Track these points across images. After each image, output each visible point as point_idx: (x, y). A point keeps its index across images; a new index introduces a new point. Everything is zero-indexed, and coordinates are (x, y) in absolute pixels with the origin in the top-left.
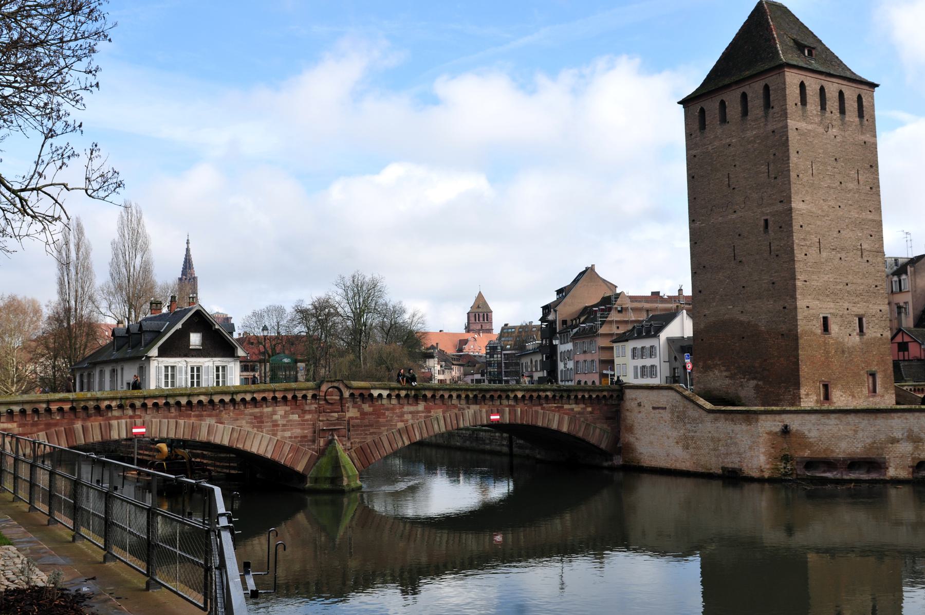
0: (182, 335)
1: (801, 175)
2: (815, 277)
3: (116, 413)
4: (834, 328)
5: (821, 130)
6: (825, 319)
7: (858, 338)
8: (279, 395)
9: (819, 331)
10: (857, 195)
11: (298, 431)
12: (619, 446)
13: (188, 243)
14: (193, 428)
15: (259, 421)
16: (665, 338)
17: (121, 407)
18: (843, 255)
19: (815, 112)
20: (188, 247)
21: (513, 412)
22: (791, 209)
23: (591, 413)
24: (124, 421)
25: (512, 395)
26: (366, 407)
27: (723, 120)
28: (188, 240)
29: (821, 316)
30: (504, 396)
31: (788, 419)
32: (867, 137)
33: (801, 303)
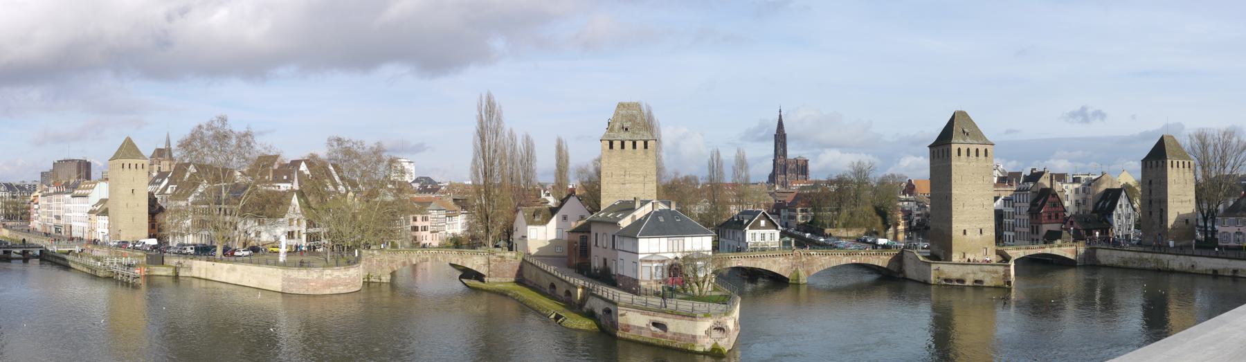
0: (758, 221)
3: (734, 259)
5: (967, 164)
6: (965, 231)
10: (982, 186)
11: (787, 265)
12: (901, 270)
13: (780, 111)
14: (755, 264)
21: (860, 258)
22: (951, 194)
26: (809, 258)
27: (938, 157)
31: (939, 265)
32: (989, 164)
33: (954, 226)
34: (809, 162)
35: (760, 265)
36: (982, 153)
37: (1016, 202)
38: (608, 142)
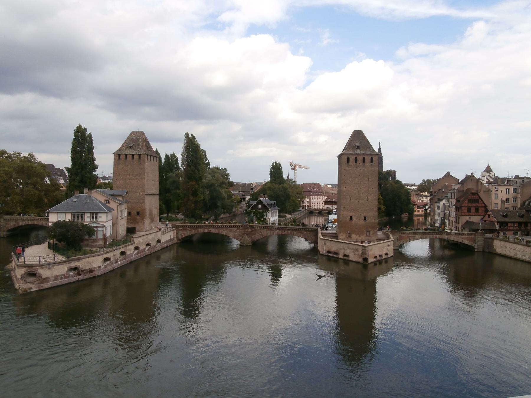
1: (345, 181)
2: (348, 207)
4: (354, 219)
5: (355, 169)
7: (363, 222)
8: (235, 226)
9: (348, 220)
10: (367, 185)
11: (238, 233)
13: (380, 144)
15: (231, 231)
16: (443, 204)
17: (206, 227)
18: (360, 201)
19: (352, 164)
20: (380, 145)
23: (310, 234)
24: (207, 229)
25: (287, 229)
26: (253, 229)
28: (380, 143)
29: (349, 216)
30: (285, 229)
31: (326, 241)
34: (397, 173)
35: (222, 232)
36: (368, 159)
37: (450, 198)
38: (117, 155)
